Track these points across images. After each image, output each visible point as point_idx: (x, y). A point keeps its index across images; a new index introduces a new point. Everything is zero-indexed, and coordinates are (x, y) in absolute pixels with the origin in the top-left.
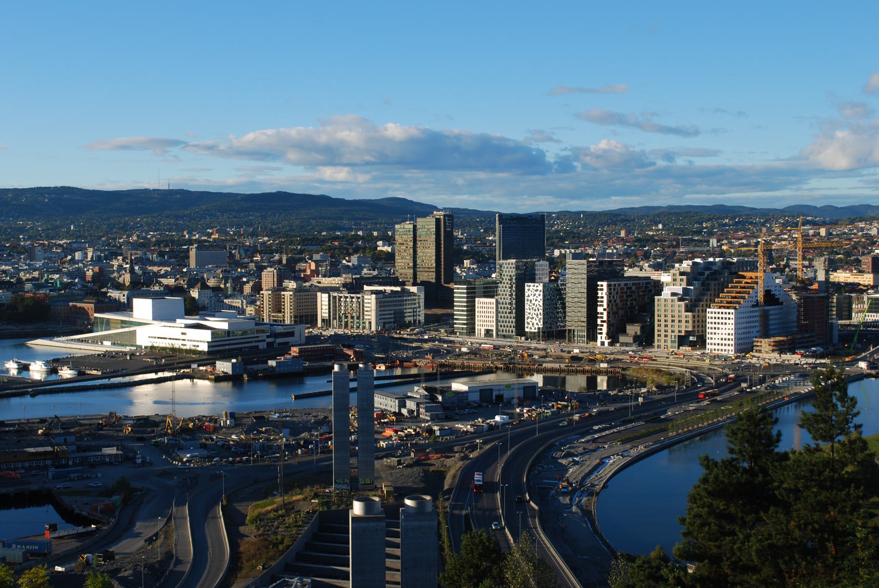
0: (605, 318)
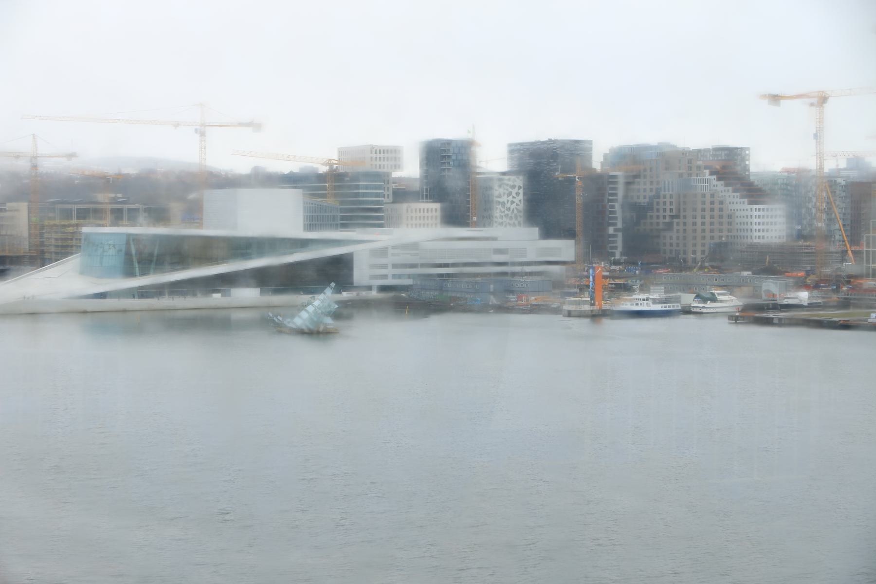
0: (620, 225)
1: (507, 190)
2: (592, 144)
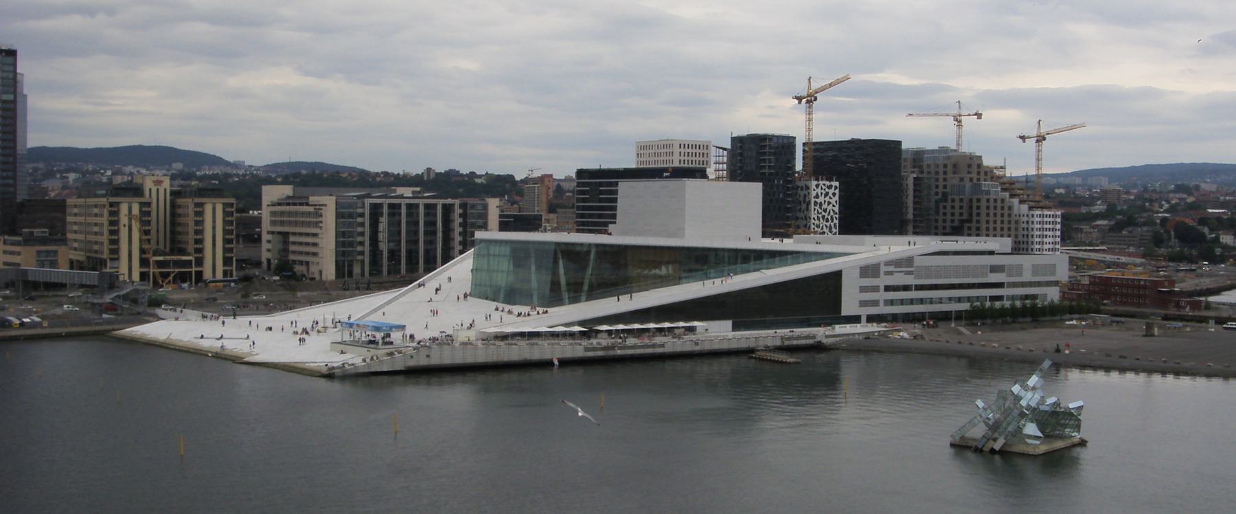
1: (825, 190)
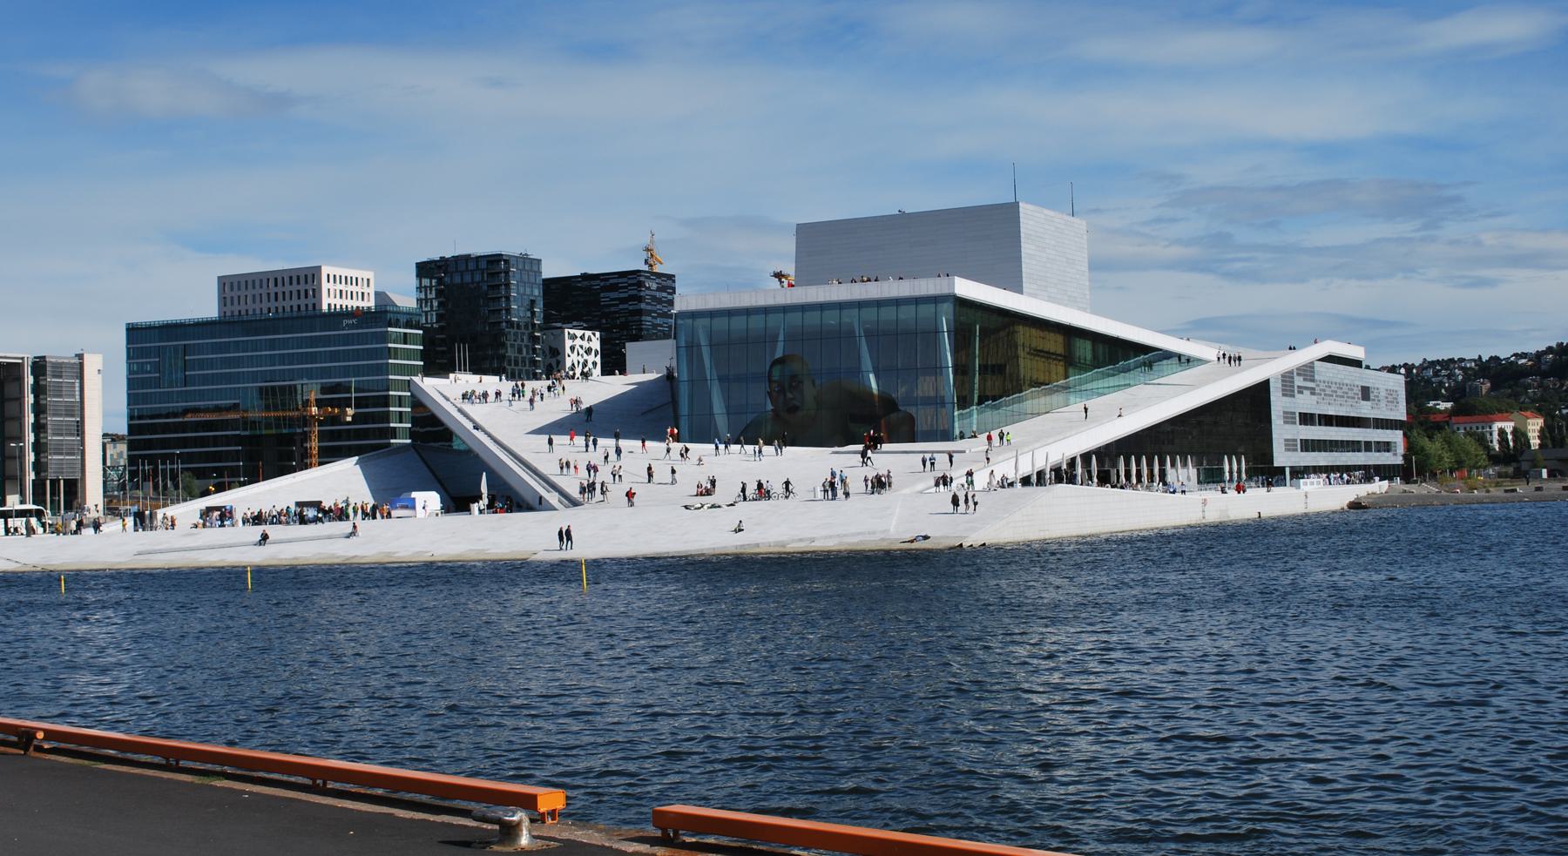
1: (582, 356)
2: (674, 281)
